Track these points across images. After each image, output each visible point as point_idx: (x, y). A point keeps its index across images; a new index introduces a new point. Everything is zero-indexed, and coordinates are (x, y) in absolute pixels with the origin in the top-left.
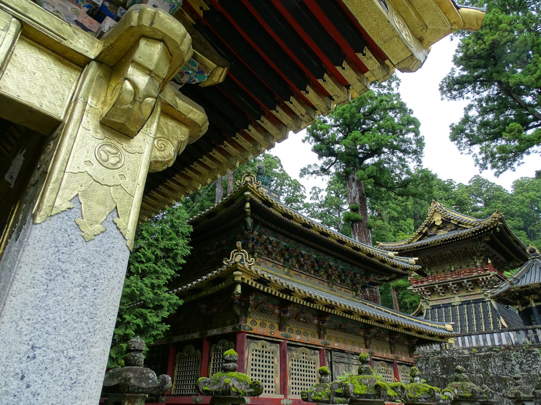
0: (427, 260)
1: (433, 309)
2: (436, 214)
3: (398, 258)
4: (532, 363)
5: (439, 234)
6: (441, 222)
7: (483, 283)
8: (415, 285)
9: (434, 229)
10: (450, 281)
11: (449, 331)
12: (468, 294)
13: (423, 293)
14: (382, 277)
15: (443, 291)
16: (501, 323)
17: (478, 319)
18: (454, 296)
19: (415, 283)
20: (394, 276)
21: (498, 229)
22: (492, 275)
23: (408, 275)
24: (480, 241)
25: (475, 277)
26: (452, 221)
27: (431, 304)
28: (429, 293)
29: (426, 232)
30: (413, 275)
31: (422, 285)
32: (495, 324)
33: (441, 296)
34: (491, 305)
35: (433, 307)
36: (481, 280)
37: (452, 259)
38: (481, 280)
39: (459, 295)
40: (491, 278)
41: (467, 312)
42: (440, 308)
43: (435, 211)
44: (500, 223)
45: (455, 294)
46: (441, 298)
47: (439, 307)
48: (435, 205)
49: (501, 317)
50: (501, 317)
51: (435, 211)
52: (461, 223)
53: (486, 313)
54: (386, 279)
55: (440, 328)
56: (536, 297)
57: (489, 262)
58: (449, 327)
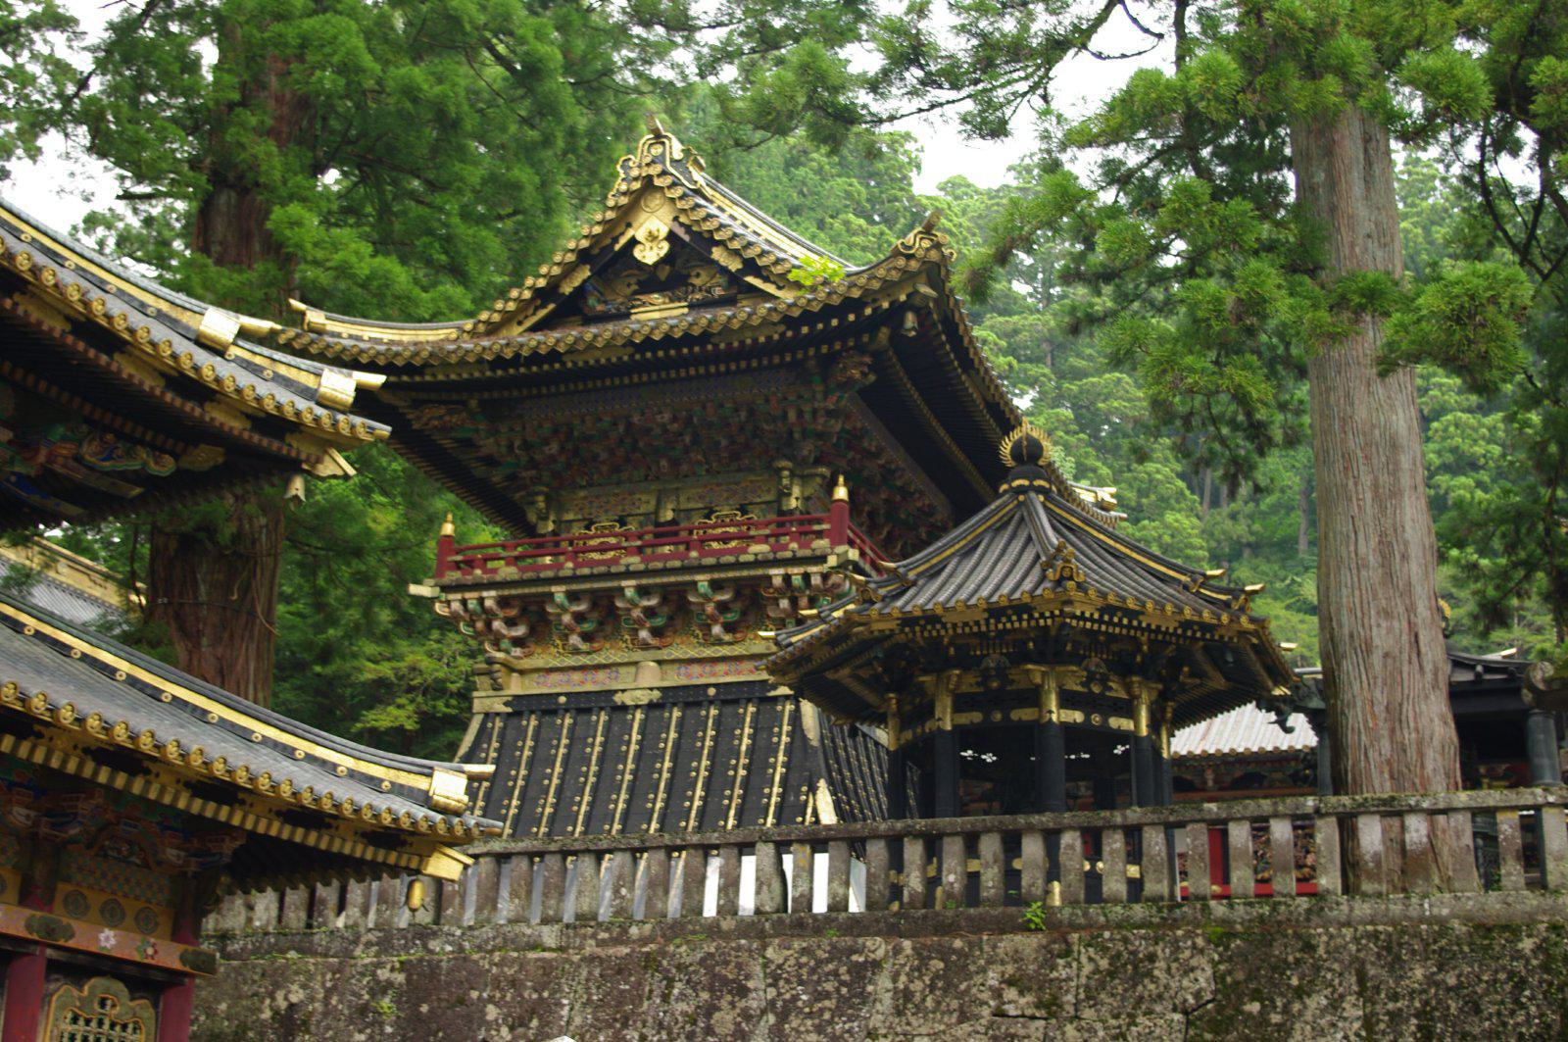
0: (554, 448)
1: (517, 714)
2: (656, 201)
3: (260, 356)
4: (837, 1012)
6: (665, 247)
7: (784, 603)
8: (453, 576)
9: (624, 289)
10: (628, 574)
11: (443, 810)
12: (708, 652)
13: (488, 625)
14: (130, 455)
15: (587, 627)
16: (815, 813)
17: (715, 785)
18: (637, 656)
19: (457, 566)
20: (204, 457)
21: (910, 320)
22: (832, 561)
23: (292, 466)
24: (825, 380)
25: (757, 563)
26: (717, 254)
27: (516, 686)
28: (520, 631)
29: (580, 292)
30: (326, 469)
31: (486, 578)
32: (790, 809)
33: (576, 651)
34: (796, 718)
35: (522, 706)
36: (777, 581)
37: (675, 463)
38: (777, 581)
39: (664, 654)
40: (825, 577)
41: (677, 745)
42: (553, 712)
43: (648, 184)
44: (925, 290)
45: (645, 646)
46: (571, 661)
47: (545, 707)
48: (657, 150)
49: (822, 784)
50: (822, 784)
51: (648, 184)
53: (760, 754)
54: (154, 469)
55: (399, 790)
56: (970, 683)
57: (841, 493)
58: (448, 784)
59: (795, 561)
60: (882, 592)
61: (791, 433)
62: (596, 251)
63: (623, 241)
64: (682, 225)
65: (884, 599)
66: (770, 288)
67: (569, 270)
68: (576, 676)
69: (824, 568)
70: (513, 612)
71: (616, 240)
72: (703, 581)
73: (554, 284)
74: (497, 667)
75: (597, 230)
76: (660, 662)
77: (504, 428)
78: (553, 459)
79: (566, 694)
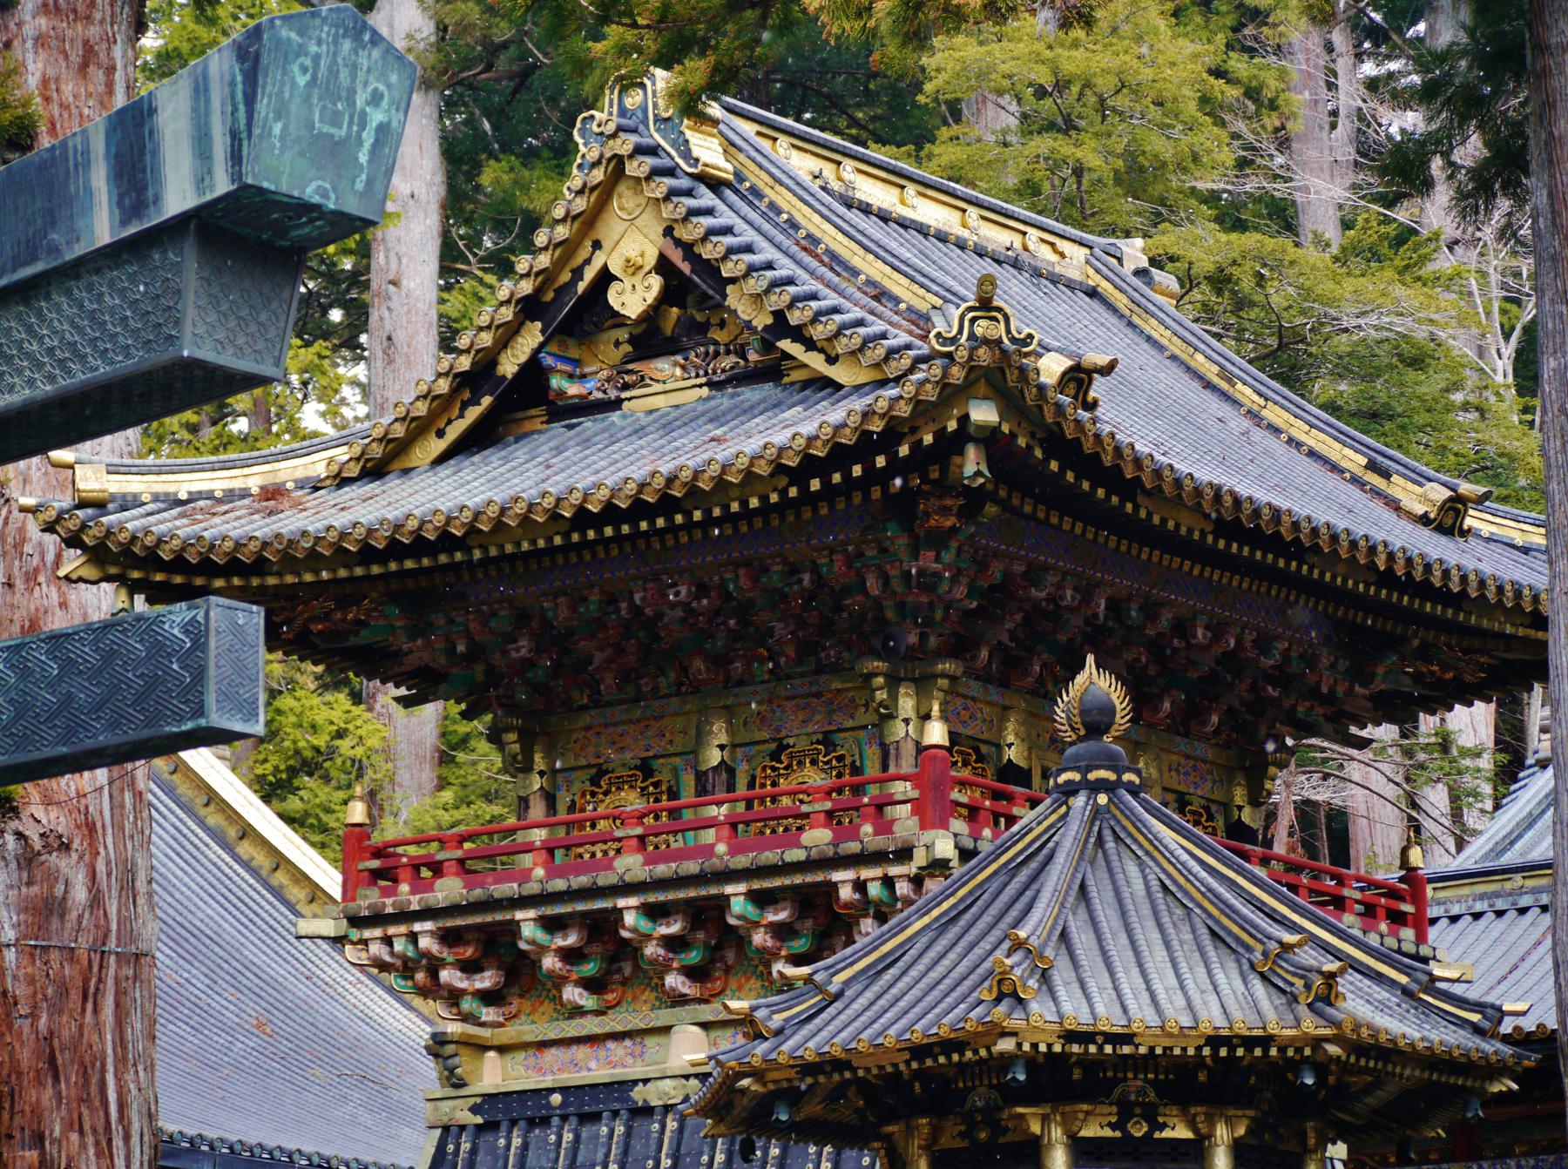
0: (523, 648)
1: (490, 1127)
2: (625, 201)
5: (638, 405)
6: (656, 282)
9: (611, 349)
15: (589, 969)
18: (663, 1017)
22: (920, 858)
28: (486, 980)
29: (533, 370)
33: (577, 1012)
37: (720, 661)
38: (846, 893)
42: (545, 1122)
45: (680, 1000)
46: (574, 1028)
52: (798, 334)
59: (878, 858)
60: (777, 1020)
61: (878, 606)
62: (550, 296)
63: (589, 274)
64: (678, 242)
65: (779, 1032)
66: (816, 361)
67: (507, 335)
68: (581, 1052)
69: (912, 868)
70: (469, 952)
71: (578, 274)
72: (735, 889)
73: (486, 364)
74: (450, 1049)
75: (544, 260)
76: (706, 1026)
77: (440, 620)
78: (529, 663)
79: (563, 1090)
